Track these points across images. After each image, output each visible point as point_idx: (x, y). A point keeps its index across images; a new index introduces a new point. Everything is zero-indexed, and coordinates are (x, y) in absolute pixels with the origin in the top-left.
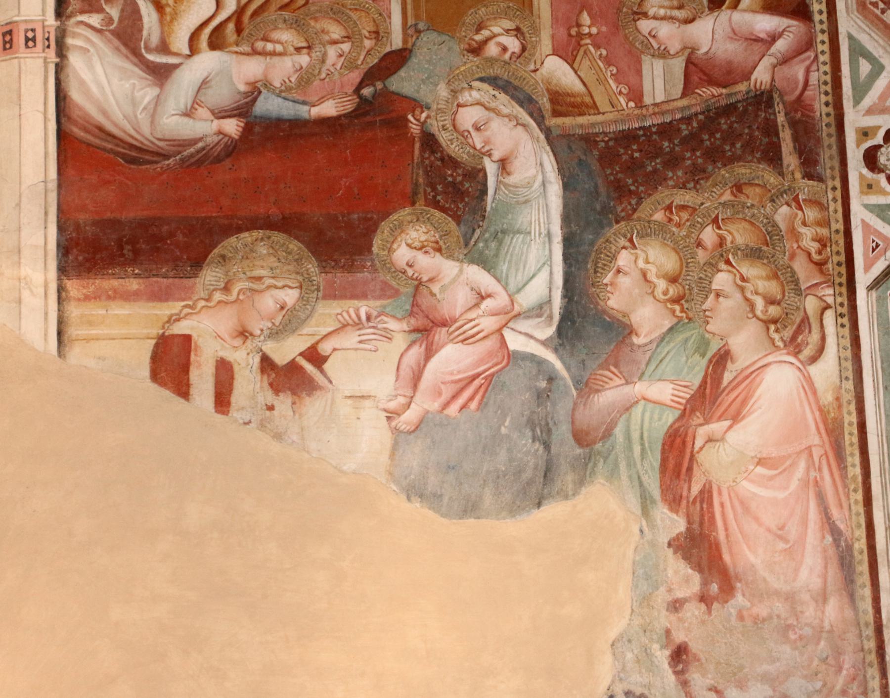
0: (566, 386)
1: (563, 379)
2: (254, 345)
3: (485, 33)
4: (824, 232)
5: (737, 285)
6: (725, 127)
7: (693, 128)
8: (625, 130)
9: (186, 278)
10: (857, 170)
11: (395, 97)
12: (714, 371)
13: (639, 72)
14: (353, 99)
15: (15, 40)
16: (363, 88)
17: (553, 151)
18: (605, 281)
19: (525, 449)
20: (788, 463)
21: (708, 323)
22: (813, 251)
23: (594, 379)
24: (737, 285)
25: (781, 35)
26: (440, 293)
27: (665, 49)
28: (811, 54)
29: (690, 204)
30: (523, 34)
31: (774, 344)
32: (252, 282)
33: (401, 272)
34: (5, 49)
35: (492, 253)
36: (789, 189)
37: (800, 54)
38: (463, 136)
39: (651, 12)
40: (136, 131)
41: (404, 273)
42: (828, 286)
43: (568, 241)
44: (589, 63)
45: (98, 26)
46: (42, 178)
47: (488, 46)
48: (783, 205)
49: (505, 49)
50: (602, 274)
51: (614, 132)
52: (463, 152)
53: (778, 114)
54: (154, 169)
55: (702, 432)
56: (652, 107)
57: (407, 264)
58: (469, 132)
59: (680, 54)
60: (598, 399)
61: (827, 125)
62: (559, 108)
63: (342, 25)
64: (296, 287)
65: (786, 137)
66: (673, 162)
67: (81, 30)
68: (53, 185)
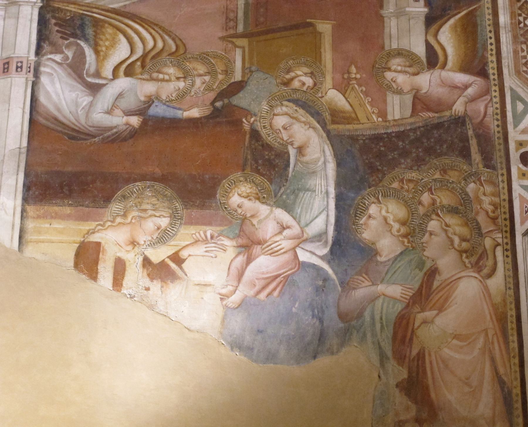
0: (334, 284)
1: (333, 280)
2: (140, 250)
3: (292, 74)
4: (497, 200)
5: (443, 229)
6: (436, 135)
7: (417, 135)
8: (376, 134)
9: (100, 208)
10: (516, 165)
11: (236, 108)
12: (428, 279)
13: (385, 101)
14: (209, 108)
15: (10, 68)
16: (216, 102)
17: (331, 144)
18: (360, 223)
19: (307, 322)
20: (473, 337)
21: (424, 250)
22: (490, 211)
23: (353, 281)
24: (443, 229)
25: (470, 85)
26: (258, 224)
27: (400, 89)
28: (488, 97)
29: (415, 179)
30: (315, 76)
31: (465, 266)
32: (141, 213)
33: (234, 211)
34: (4, 72)
35: (291, 202)
36: (475, 174)
37: (482, 97)
38: (276, 133)
39: (393, 68)
40: (76, 120)
41: (236, 211)
42: (499, 232)
43: (339, 199)
44: (355, 94)
45: (60, 61)
46: (18, 146)
47: (293, 82)
48: (471, 182)
49: (304, 84)
50: (359, 217)
51: (369, 135)
52: (275, 142)
53: (469, 130)
54: (86, 144)
55: (420, 317)
56: (392, 121)
57: (238, 206)
58: (280, 130)
59: (410, 92)
60: (355, 294)
61: (498, 138)
62: (335, 119)
63: (206, 66)
64: (168, 217)
65: (473, 143)
66: (405, 154)
67: (49, 63)
68: (24, 150)
